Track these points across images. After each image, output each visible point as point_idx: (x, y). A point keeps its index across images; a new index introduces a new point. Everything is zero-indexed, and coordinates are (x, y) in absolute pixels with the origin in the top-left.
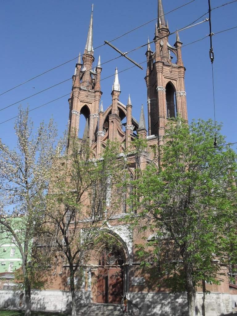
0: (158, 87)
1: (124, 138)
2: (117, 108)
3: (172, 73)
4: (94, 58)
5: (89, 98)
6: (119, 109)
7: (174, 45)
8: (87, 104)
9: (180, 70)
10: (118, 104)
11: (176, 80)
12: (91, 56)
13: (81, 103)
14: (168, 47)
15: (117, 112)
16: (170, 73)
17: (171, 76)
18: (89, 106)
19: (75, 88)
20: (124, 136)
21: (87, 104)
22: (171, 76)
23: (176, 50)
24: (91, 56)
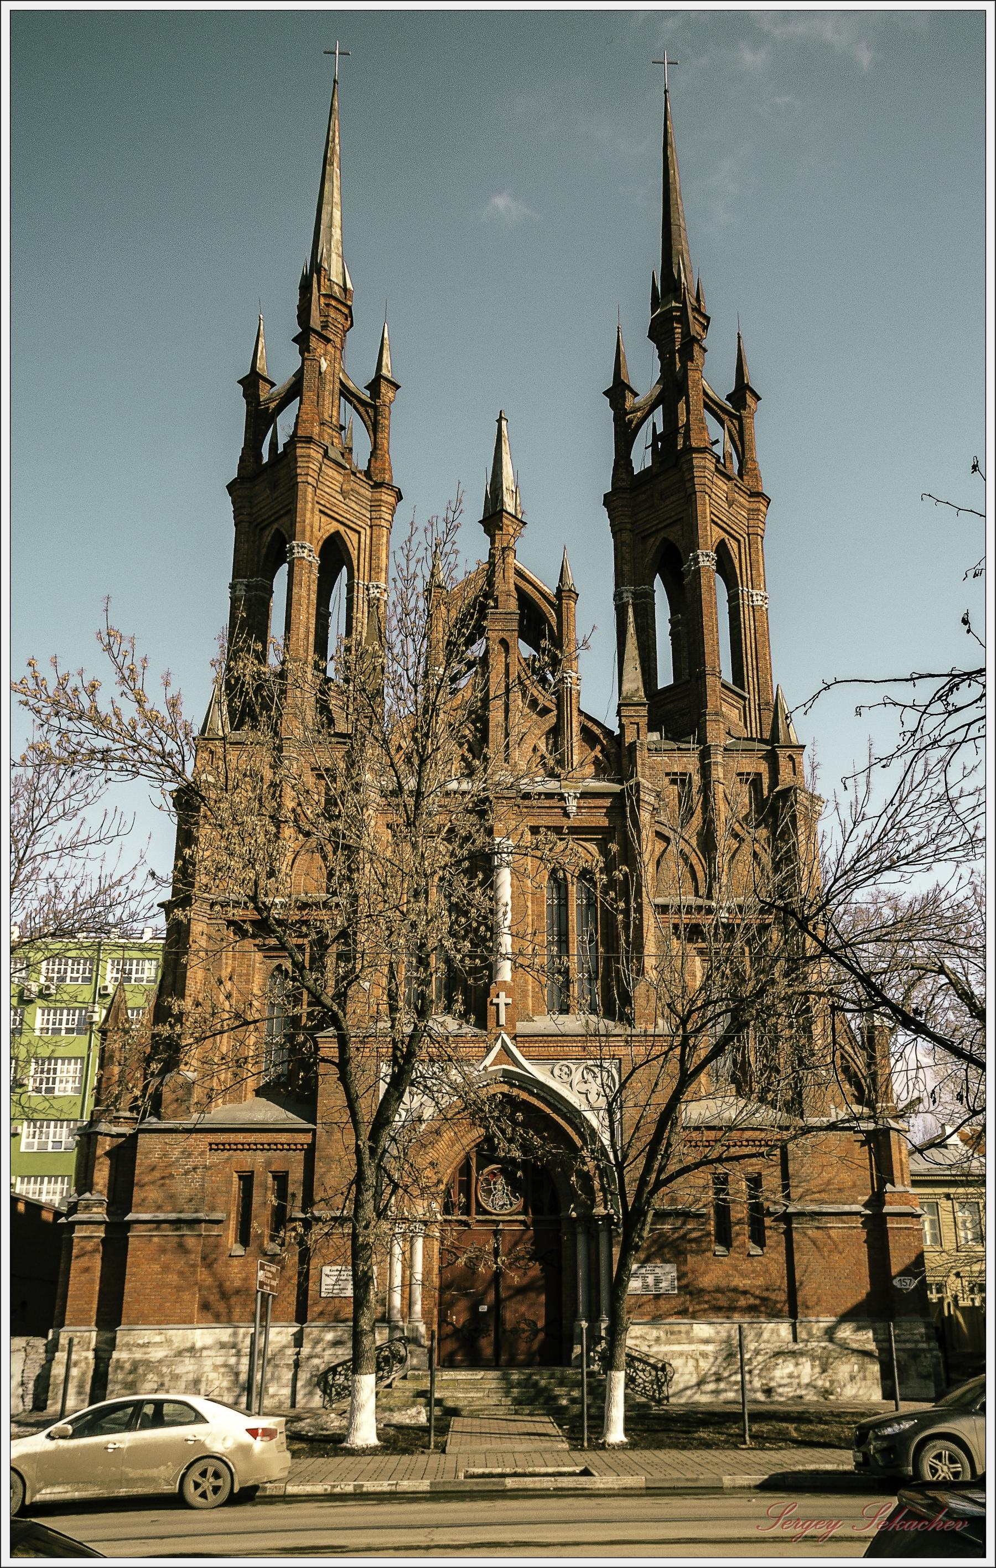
0: (699, 552)
1: (551, 719)
2: (512, 587)
3: (731, 510)
4: (352, 325)
5: (353, 505)
6: (523, 599)
7: (729, 398)
8: (342, 529)
9: (755, 506)
10: (519, 573)
11: (738, 541)
12: (346, 311)
13: (324, 518)
14: (705, 393)
15: (513, 605)
16: (725, 505)
17: (729, 519)
18: (351, 539)
19: (309, 442)
20: (550, 711)
21: (342, 529)
22: (729, 519)
23: (740, 419)
24: (346, 311)
